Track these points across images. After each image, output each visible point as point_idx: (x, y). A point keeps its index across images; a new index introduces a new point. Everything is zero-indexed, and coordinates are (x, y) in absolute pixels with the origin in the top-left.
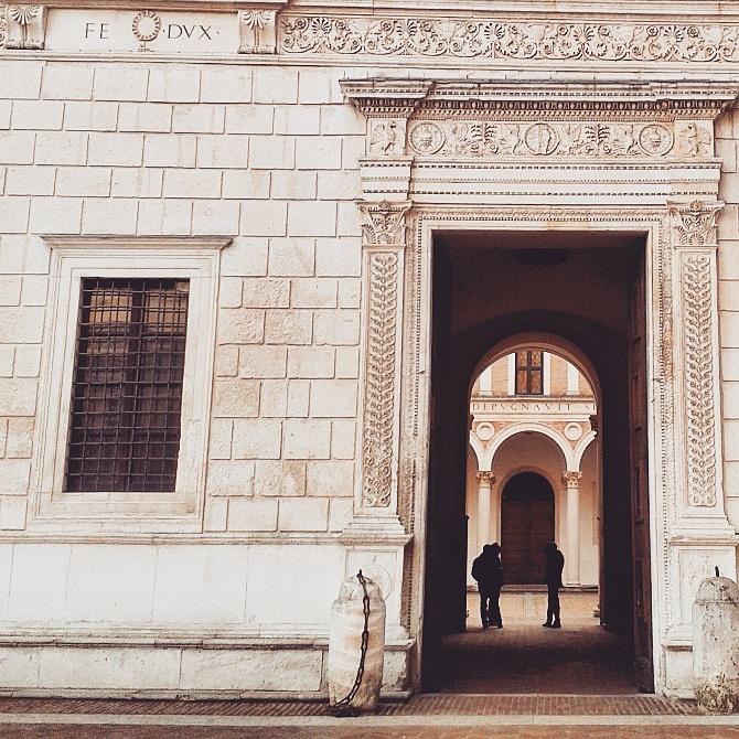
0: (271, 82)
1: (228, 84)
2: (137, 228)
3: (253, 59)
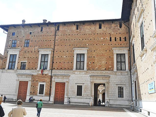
0: (86, 75)
1: (84, 75)
2: (80, 83)
3: (85, 74)
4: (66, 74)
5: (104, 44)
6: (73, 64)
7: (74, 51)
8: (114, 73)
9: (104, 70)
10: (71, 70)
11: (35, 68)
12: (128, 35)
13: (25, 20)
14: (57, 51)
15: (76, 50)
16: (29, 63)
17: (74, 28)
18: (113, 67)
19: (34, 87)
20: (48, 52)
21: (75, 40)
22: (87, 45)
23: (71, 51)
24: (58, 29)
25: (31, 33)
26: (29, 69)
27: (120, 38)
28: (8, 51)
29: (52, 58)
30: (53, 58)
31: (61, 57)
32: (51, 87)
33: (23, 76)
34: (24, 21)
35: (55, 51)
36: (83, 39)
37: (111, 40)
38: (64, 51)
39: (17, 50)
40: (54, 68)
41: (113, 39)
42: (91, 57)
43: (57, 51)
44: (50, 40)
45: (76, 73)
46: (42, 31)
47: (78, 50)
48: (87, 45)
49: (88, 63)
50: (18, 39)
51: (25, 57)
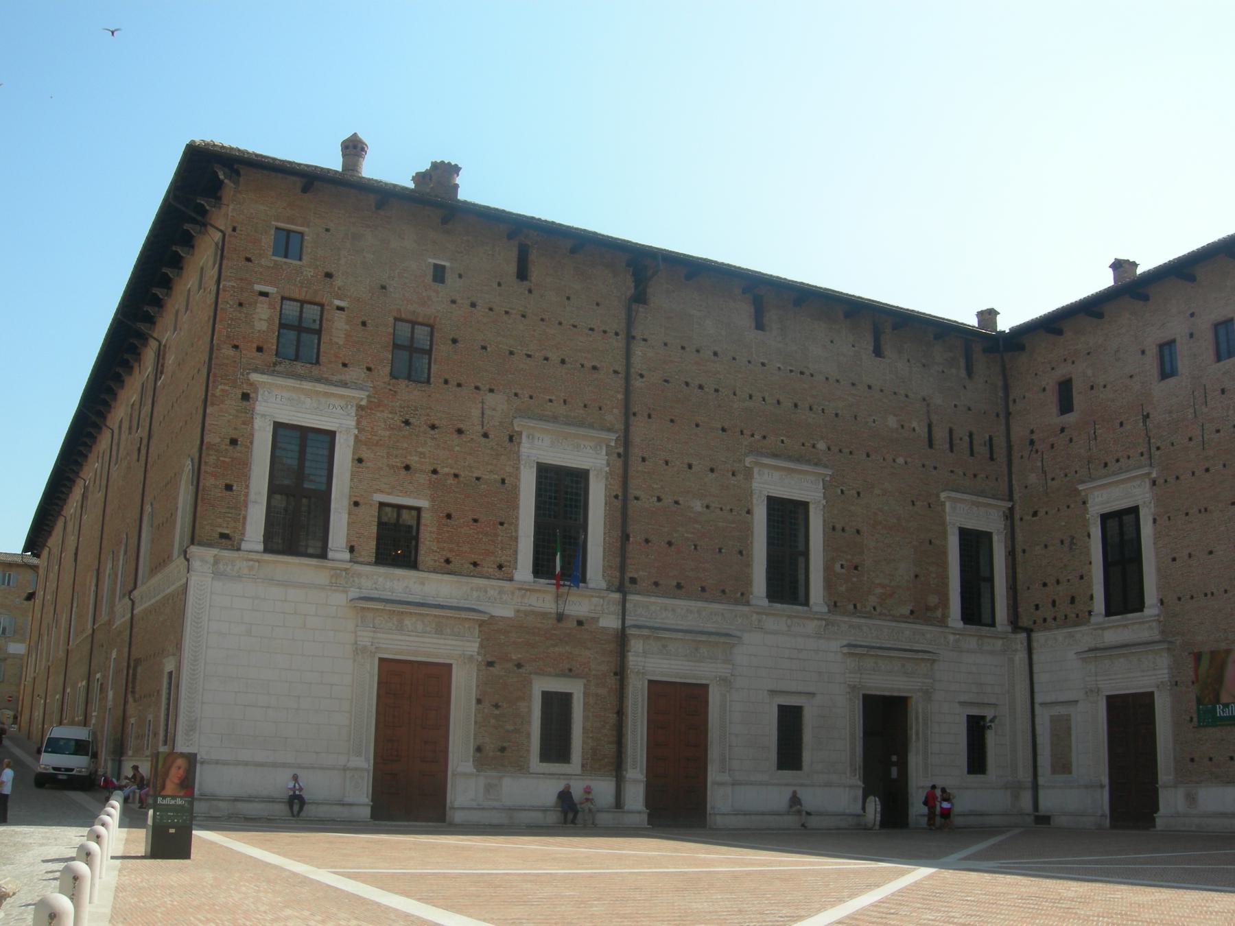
4: (710, 627)
5: (901, 460)
6: (749, 565)
7: (749, 474)
8: (951, 638)
9: (902, 616)
10: (737, 602)
11: (500, 567)
12: (1003, 428)
13: (362, 136)
14: (644, 460)
15: (766, 471)
16: (449, 516)
17: (742, 315)
18: (944, 603)
19: (497, 706)
20: (587, 454)
21: (751, 397)
22: (821, 446)
23: (733, 475)
24: (640, 297)
25: (439, 274)
26: (447, 566)
27: (971, 435)
28: (246, 389)
29: (618, 503)
30: (622, 502)
31: (677, 502)
32: (620, 713)
33: (408, 622)
34: (353, 148)
35: (636, 452)
36: (796, 406)
37: (931, 445)
38: (690, 466)
39: (342, 397)
40: (633, 581)
41: (940, 434)
42: (843, 530)
43: (644, 460)
44: (594, 368)
45: (770, 623)
46: (522, 274)
47: (777, 475)
48: (821, 446)
49: (828, 568)
50: (338, 303)
51: (407, 468)
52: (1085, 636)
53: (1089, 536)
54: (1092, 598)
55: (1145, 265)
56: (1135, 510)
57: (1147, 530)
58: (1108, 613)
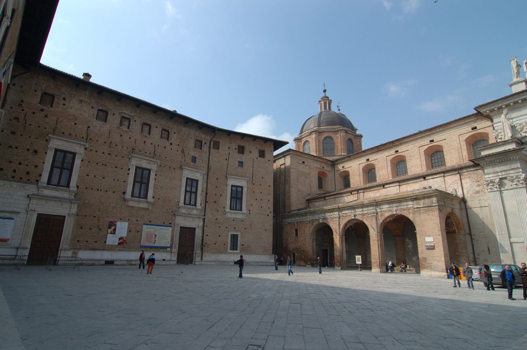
52: (32, 189)
53: (46, 153)
54: (40, 175)
55: (92, 80)
56: (74, 154)
57: (78, 162)
58: (49, 182)
